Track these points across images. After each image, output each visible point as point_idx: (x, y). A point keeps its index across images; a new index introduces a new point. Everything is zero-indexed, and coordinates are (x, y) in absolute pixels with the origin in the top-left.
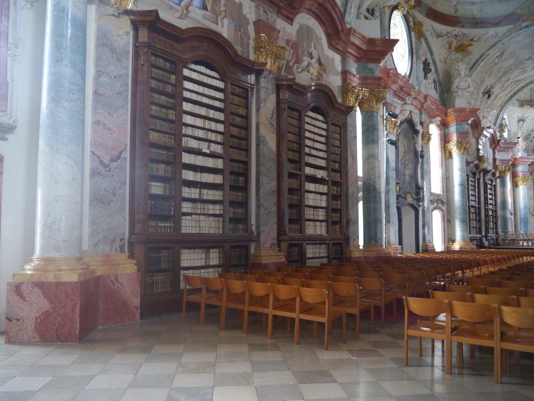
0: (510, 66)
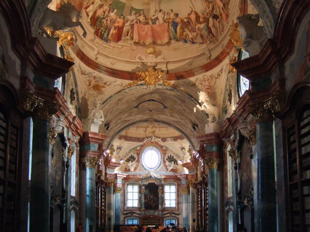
0: (124, 110)
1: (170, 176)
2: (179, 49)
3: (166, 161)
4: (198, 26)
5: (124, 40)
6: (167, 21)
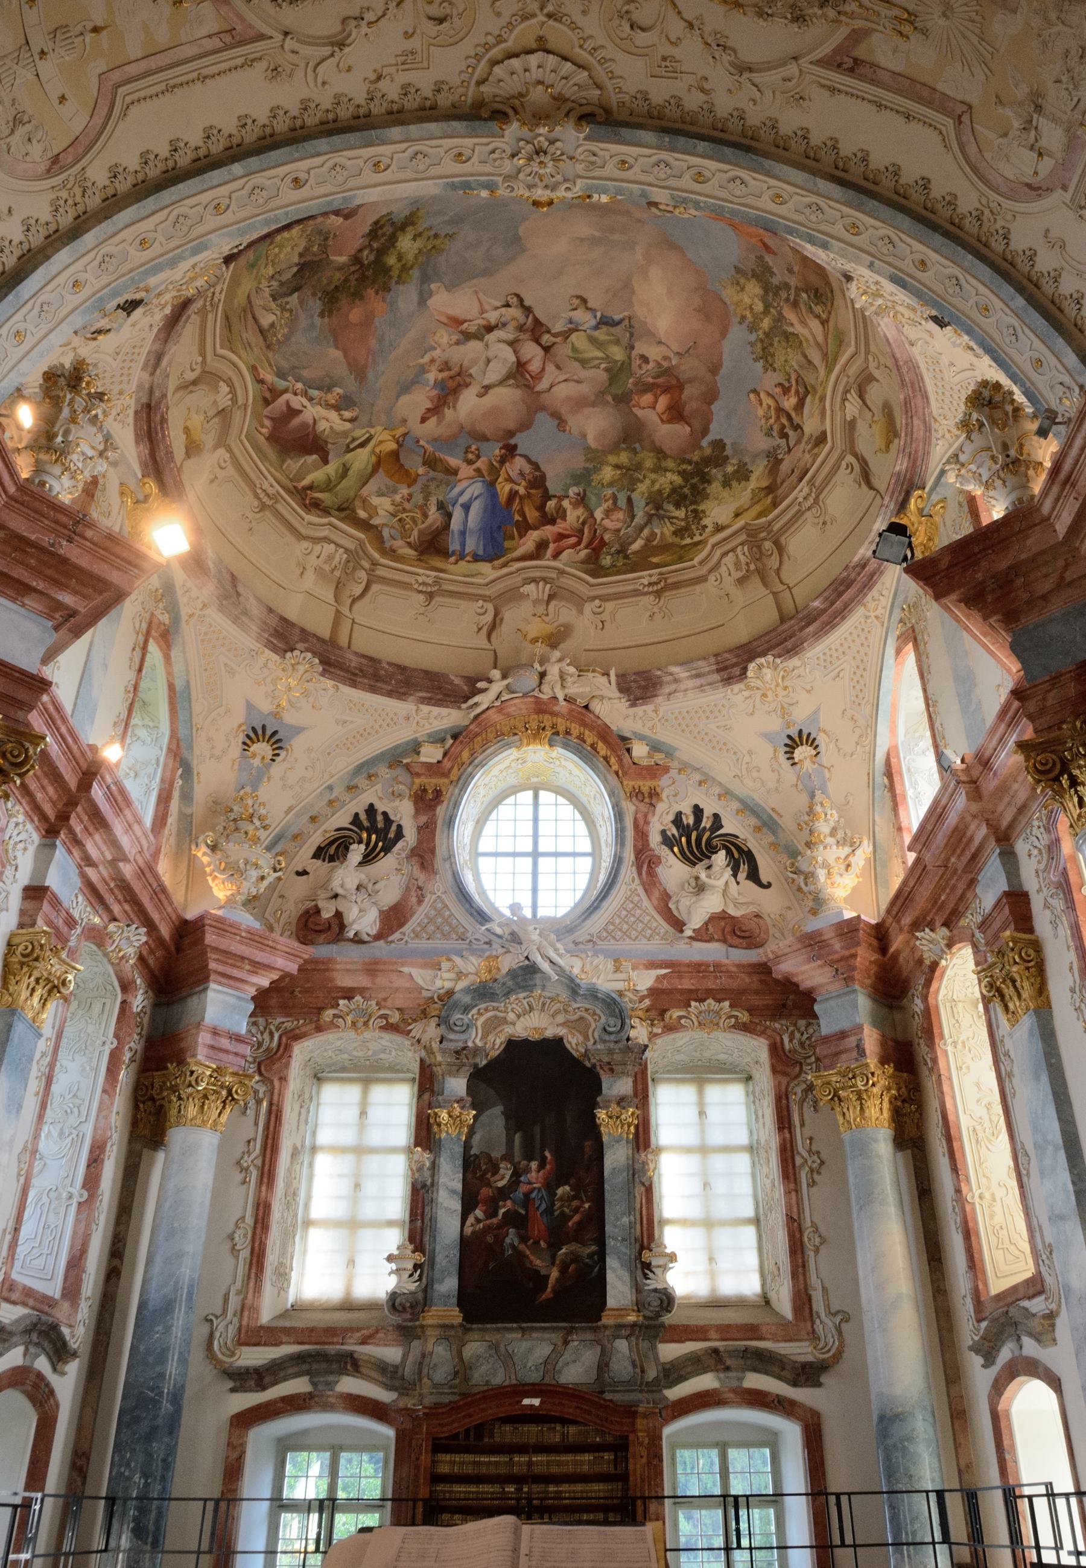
1: (699, 968)
3: (664, 851)
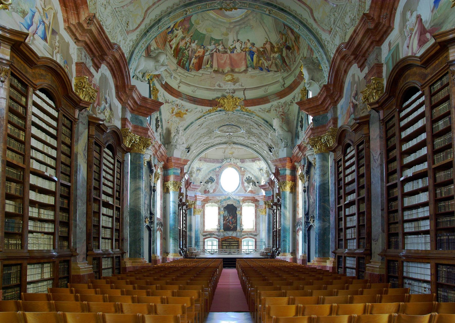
2: (255, 76)
3: (245, 182)
4: (273, 55)
5: (205, 69)
6: (244, 50)
